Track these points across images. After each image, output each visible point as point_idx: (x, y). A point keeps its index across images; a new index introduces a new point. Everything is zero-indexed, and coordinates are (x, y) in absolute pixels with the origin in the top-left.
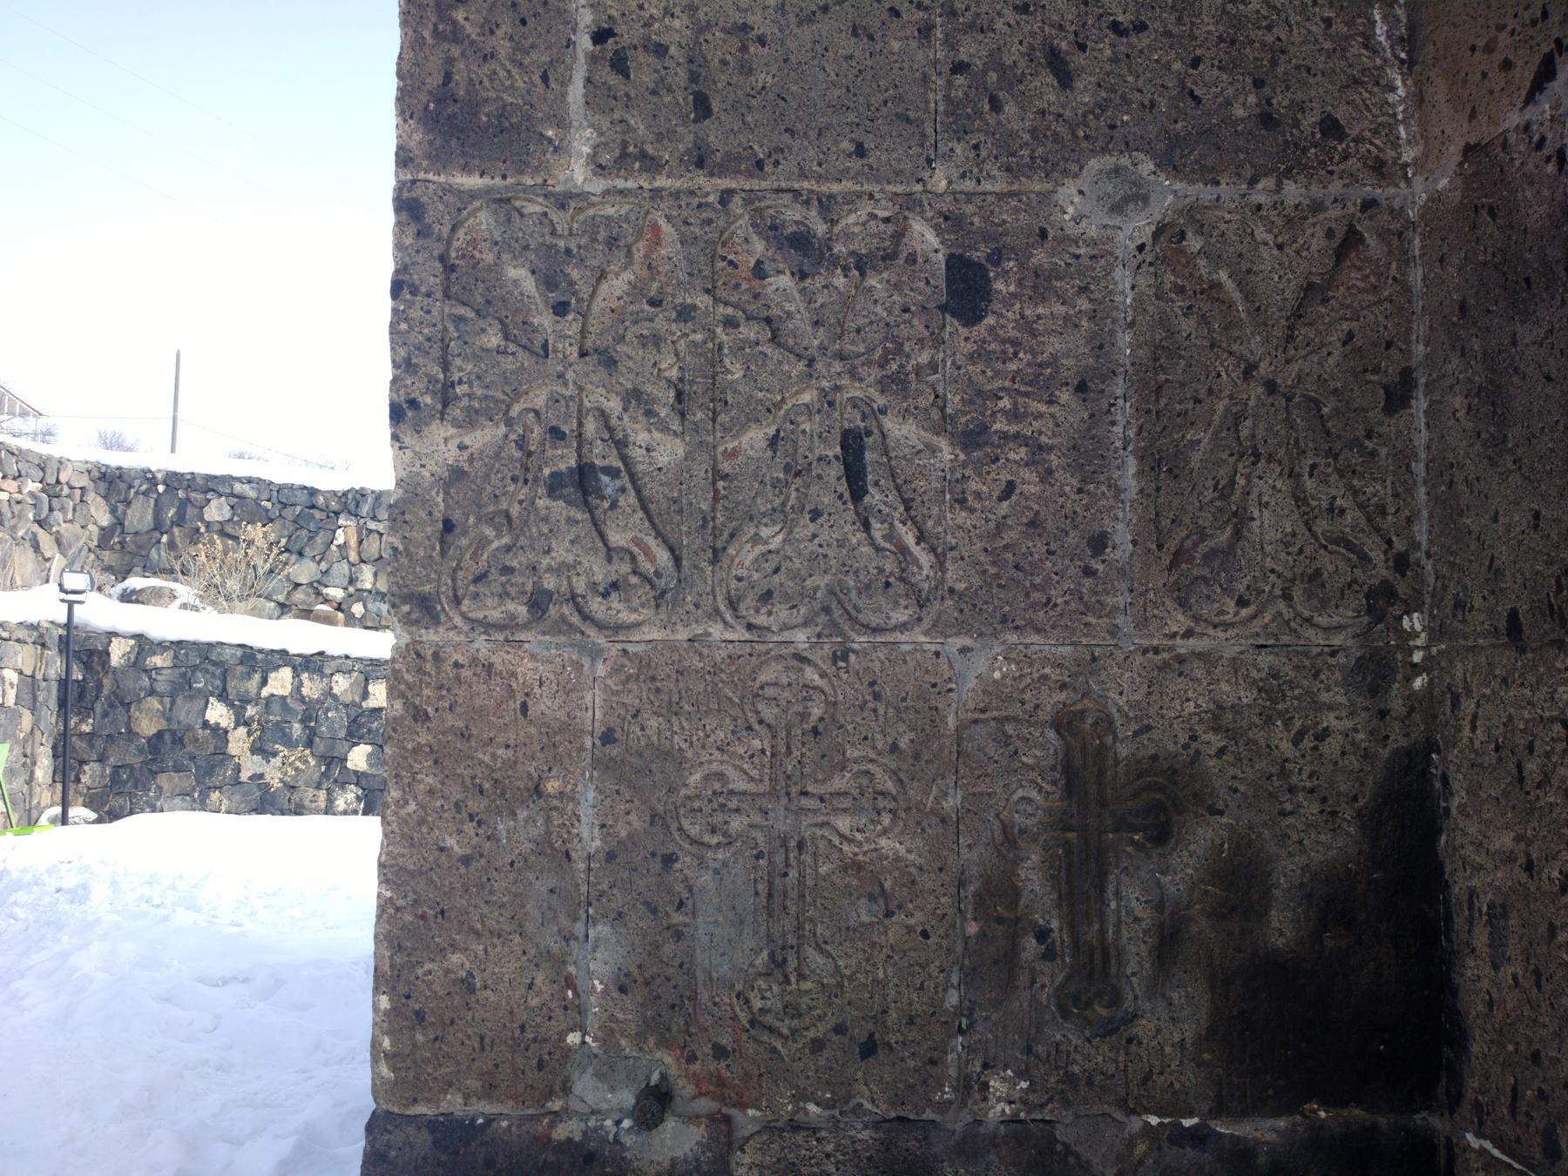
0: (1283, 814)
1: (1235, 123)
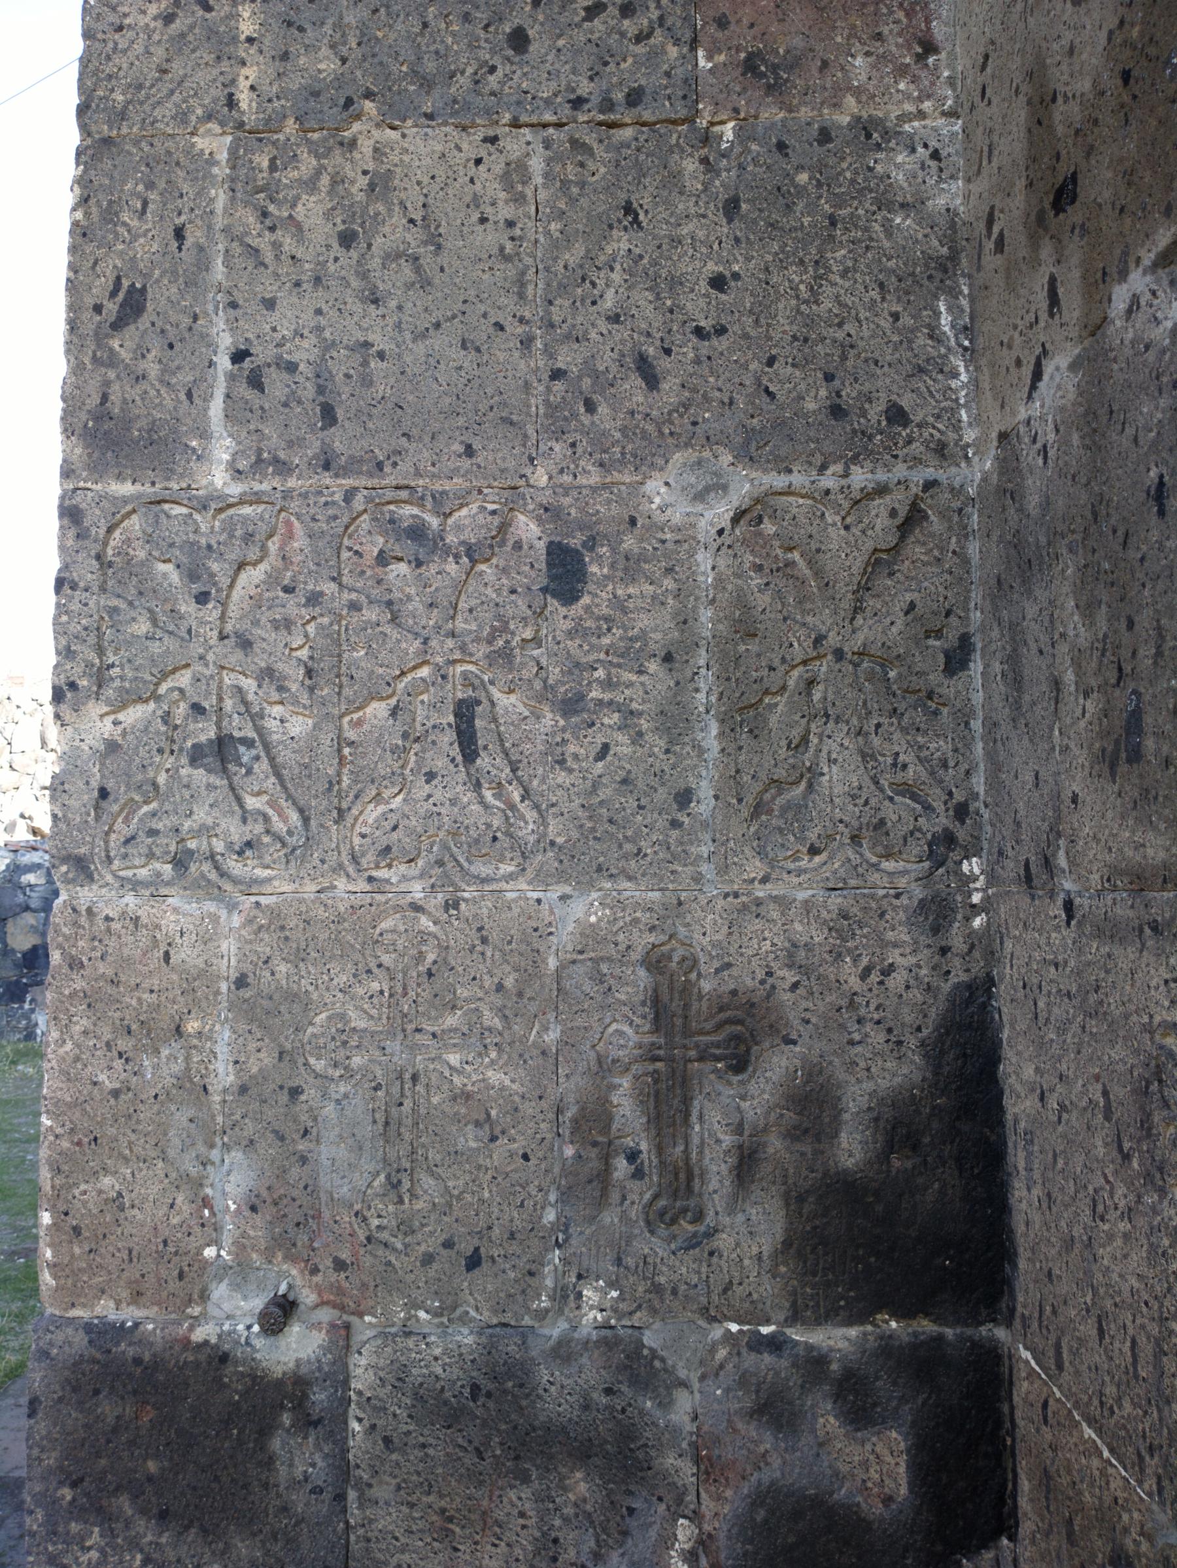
0: (851, 1043)
1: (806, 416)
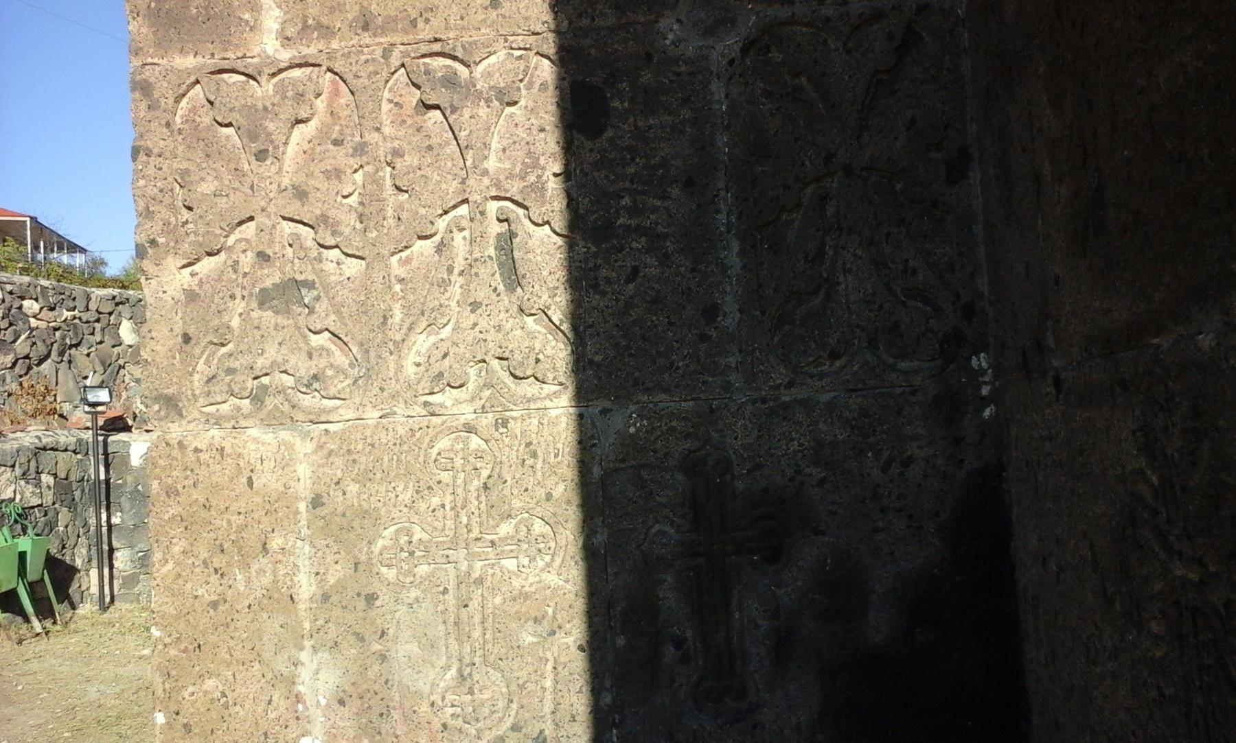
0: (876, 530)
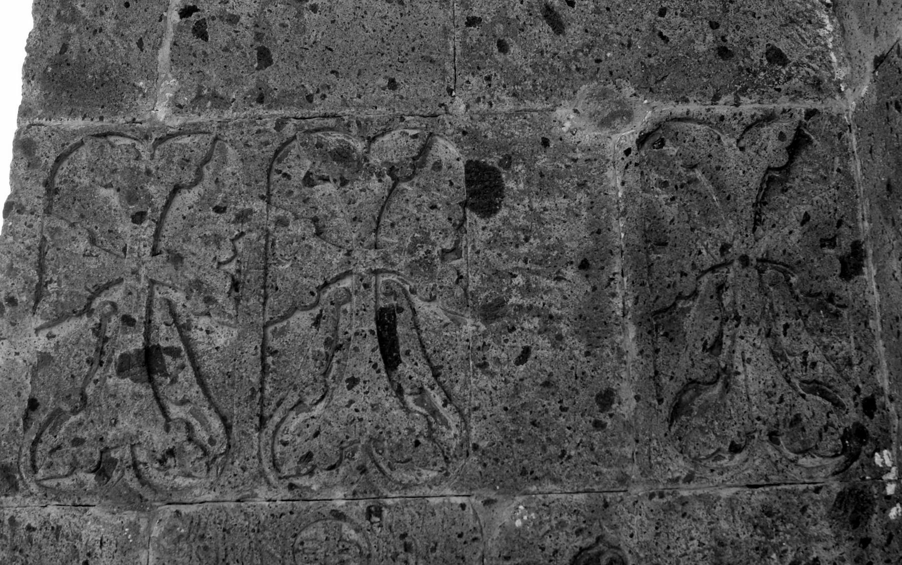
1: (697, 55)
